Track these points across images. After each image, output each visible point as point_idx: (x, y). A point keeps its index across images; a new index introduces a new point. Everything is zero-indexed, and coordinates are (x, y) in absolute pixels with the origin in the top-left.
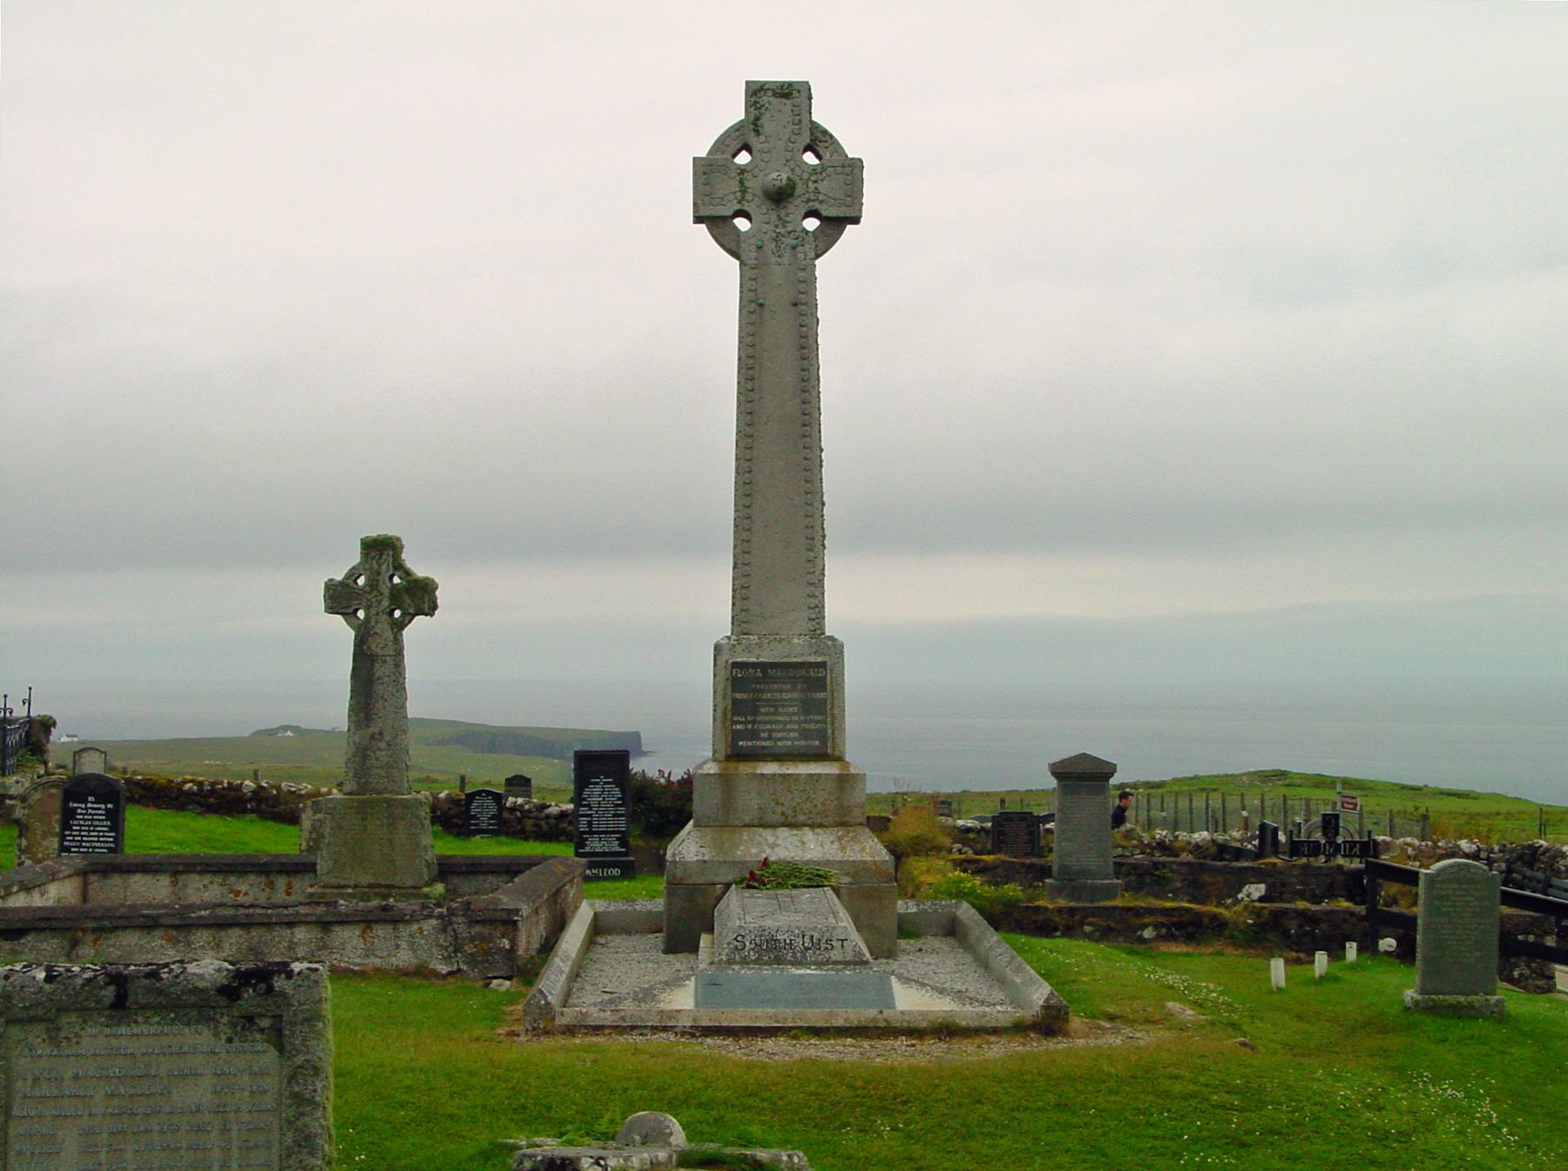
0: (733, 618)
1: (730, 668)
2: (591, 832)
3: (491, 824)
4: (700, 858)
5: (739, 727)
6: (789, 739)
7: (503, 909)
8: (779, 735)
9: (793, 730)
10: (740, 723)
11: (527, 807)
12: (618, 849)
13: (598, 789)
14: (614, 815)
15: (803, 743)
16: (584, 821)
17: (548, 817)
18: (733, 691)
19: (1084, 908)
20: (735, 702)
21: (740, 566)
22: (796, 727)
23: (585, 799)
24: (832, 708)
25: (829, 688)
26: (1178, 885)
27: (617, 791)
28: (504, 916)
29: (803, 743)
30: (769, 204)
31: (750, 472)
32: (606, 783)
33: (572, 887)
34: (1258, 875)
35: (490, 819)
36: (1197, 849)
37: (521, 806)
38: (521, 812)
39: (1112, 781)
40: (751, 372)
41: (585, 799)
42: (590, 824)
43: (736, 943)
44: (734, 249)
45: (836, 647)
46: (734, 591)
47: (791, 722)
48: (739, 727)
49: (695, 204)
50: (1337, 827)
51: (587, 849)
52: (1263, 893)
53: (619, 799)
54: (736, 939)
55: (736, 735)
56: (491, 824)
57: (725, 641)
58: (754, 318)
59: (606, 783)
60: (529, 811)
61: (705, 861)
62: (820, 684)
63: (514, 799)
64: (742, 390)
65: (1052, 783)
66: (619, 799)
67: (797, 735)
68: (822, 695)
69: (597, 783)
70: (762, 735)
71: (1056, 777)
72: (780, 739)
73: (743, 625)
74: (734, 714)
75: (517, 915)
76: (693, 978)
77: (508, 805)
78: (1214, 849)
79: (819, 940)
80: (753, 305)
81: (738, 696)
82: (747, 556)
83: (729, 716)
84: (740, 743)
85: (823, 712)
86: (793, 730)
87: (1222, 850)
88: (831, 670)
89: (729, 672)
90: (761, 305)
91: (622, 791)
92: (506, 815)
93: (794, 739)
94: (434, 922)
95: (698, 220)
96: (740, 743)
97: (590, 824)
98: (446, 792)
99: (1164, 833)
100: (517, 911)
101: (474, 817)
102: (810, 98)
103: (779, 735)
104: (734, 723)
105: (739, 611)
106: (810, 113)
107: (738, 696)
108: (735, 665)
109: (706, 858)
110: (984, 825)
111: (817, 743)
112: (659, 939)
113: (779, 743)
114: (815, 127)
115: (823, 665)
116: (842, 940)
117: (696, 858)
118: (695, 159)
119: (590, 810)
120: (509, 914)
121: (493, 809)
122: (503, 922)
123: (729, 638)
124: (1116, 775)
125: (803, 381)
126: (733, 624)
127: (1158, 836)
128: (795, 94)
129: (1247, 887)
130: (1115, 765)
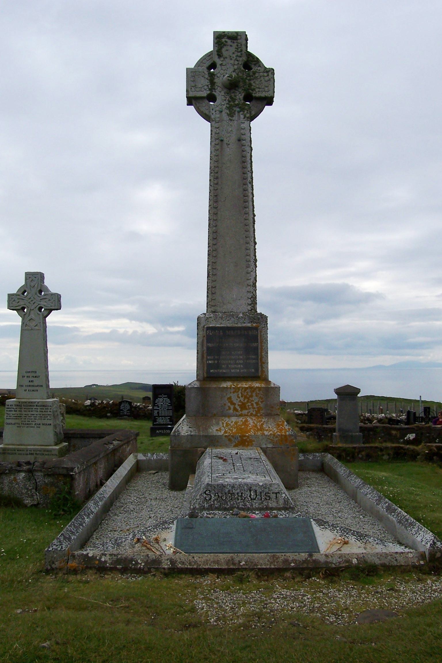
0: (207, 303)
1: (205, 330)
2: (158, 416)
3: (128, 413)
4: (189, 433)
5: (210, 362)
6: (237, 368)
7: (63, 468)
8: (233, 366)
9: (240, 364)
10: (211, 360)
11: (141, 406)
12: (169, 423)
13: (161, 400)
14: (168, 410)
15: (245, 370)
16: (156, 412)
17: (148, 410)
18: (207, 342)
19: (359, 448)
20: (208, 348)
21: (211, 276)
22: (241, 362)
23: (156, 403)
24: (261, 353)
25: (259, 340)
26: (383, 434)
27: (168, 400)
28: (65, 472)
29: (245, 370)
30: (225, 90)
31: (216, 226)
32: (164, 397)
33: (128, 446)
34: (411, 431)
35: (127, 411)
36: (380, 421)
37: (139, 406)
38: (139, 409)
39: (359, 395)
40: (216, 175)
41: (156, 403)
42: (158, 413)
43: (205, 495)
44: (207, 112)
45: (263, 319)
46: (208, 289)
47: (239, 359)
48: (210, 362)
49: (187, 91)
50: (429, 412)
51: (157, 423)
52: (414, 437)
53: (169, 403)
54: (205, 492)
55: (209, 366)
56: (128, 413)
57: (203, 316)
58: (218, 147)
59: (164, 397)
60: (142, 408)
61: (192, 435)
62: (255, 339)
63: (136, 404)
64: (212, 184)
65: (335, 397)
66: (169, 403)
67: (242, 366)
68: (255, 345)
69: (161, 397)
70: (223, 366)
71: (337, 394)
72: (233, 369)
73: (213, 308)
74: (208, 355)
75: (72, 471)
76: (175, 522)
77: (134, 406)
78: (387, 420)
79: (261, 493)
80: (217, 141)
81: (210, 345)
82: (214, 271)
83: (205, 356)
84: (211, 371)
85: (257, 354)
86: (240, 364)
87: (391, 421)
88: (261, 332)
89: (205, 332)
90: (222, 141)
91: (171, 400)
92: (133, 409)
93: (240, 369)
94: (23, 474)
95: (189, 103)
96: (211, 371)
97: (158, 413)
98: (112, 401)
99: (369, 415)
100: (72, 469)
101: (122, 410)
102: (247, 40)
103: (233, 366)
104: (207, 360)
105: (210, 300)
106: (247, 47)
107: (210, 345)
108: (208, 328)
109: (192, 434)
110: (305, 412)
111: (253, 370)
112: (165, 477)
113: (233, 371)
114: (250, 55)
115: (256, 329)
116: (276, 493)
117: (186, 434)
118: (187, 69)
119: (158, 407)
120: (67, 471)
121: (128, 407)
122: (65, 476)
123: (205, 314)
124: (360, 393)
125: (244, 173)
126: (207, 307)
127: (367, 416)
128: (239, 37)
129: (408, 435)
130: (360, 389)
